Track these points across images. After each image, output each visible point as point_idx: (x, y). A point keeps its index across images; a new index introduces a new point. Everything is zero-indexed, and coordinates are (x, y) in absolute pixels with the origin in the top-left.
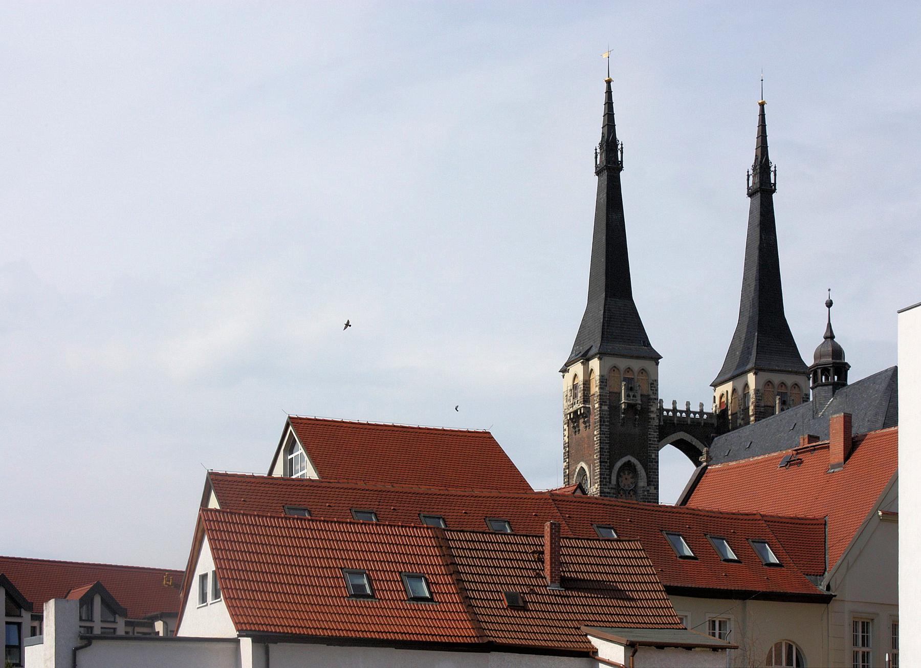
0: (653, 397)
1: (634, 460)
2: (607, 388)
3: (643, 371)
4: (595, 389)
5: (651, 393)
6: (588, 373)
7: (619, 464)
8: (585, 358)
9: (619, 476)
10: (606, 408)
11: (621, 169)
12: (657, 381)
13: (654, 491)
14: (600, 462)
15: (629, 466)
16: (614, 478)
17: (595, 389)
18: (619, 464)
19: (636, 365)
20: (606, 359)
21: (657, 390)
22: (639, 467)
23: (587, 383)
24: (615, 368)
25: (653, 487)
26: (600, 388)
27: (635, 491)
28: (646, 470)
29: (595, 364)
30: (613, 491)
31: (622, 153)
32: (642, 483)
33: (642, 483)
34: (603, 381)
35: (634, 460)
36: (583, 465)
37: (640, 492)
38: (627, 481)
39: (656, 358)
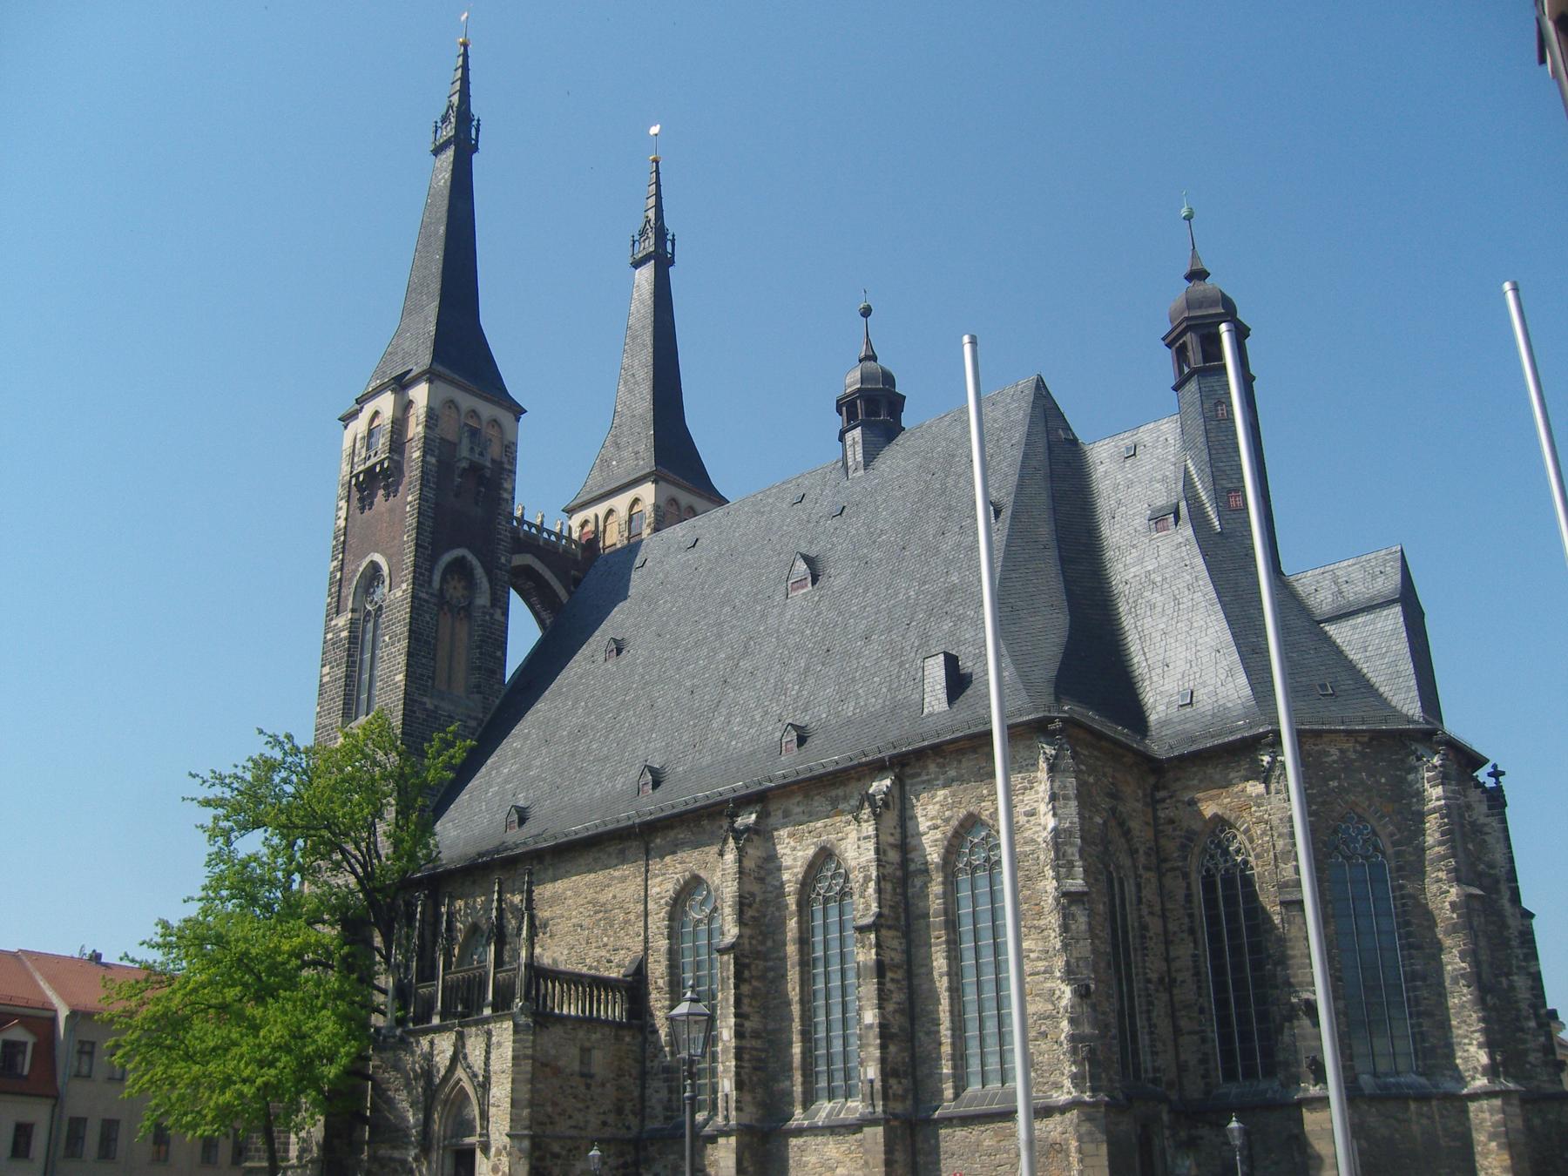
0: (507, 466)
1: (470, 557)
2: (437, 430)
3: (495, 422)
4: (415, 429)
5: (505, 459)
6: (405, 407)
7: (447, 558)
8: (401, 384)
9: (443, 580)
10: (433, 460)
11: (476, 149)
12: (515, 444)
13: (498, 616)
14: (417, 545)
15: (460, 566)
16: (437, 577)
17: (415, 429)
18: (447, 558)
19: (487, 410)
20: (438, 383)
21: (515, 459)
22: (479, 572)
23: (399, 424)
24: (451, 404)
25: (499, 611)
26: (427, 426)
27: (467, 610)
28: (490, 581)
29: (420, 394)
30: (433, 600)
31: (478, 130)
32: (483, 600)
33: (483, 600)
34: (432, 417)
35: (470, 557)
36: (378, 558)
37: (477, 614)
38: (456, 590)
39: (518, 411)
